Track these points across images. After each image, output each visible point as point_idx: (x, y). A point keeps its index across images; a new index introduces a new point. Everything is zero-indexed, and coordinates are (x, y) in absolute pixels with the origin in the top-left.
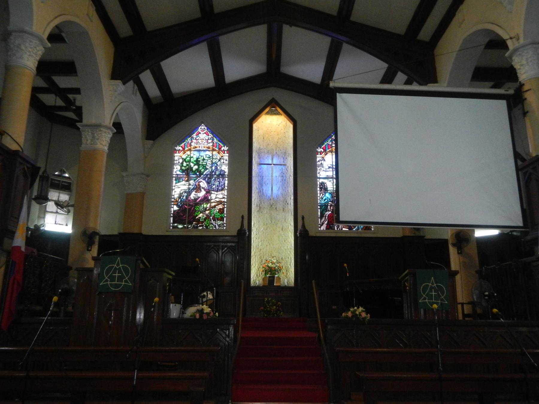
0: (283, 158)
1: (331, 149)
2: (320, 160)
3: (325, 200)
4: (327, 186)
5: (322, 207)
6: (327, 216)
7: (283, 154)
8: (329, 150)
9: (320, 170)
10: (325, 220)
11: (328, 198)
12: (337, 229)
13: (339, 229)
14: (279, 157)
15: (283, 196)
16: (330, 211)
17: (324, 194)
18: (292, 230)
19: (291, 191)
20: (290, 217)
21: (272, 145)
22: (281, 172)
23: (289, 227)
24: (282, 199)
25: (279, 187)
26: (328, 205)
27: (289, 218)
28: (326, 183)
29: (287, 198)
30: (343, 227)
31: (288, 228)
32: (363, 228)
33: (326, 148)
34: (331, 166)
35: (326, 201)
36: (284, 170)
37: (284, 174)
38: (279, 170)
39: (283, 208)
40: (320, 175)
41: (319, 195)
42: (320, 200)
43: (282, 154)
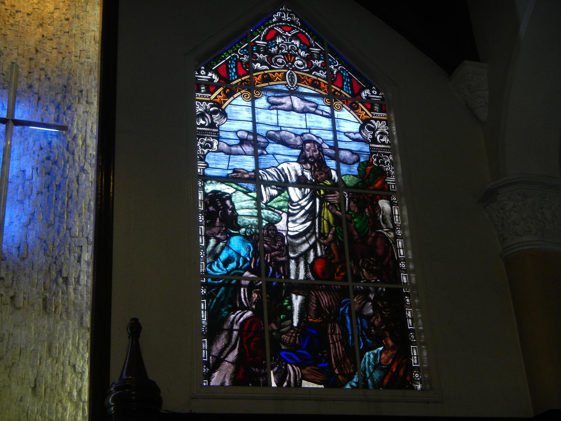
0: (58, 107)
1: (248, 77)
2: (207, 111)
3: (226, 263)
4: (234, 209)
5: (217, 292)
6: (236, 327)
7: (57, 94)
8: (240, 80)
9: (206, 147)
10: (226, 346)
11: (239, 254)
12: (280, 383)
13: (285, 384)
14: (41, 102)
15: (45, 250)
16: (248, 309)
17: (222, 241)
18: (80, 392)
19: (82, 230)
20: (71, 334)
21: (15, 55)
22: (45, 156)
23: (68, 380)
24: (40, 259)
25: (33, 214)
26: (239, 282)
27: (66, 341)
28: (230, 198)
29: (63, 258)
30: (304, 378)
31: (63, 382)
32: (382, 378)
33: (229, 73)
34: (251, 137)
35: (232, 265)
36: (56, 151)
37: (55, 163)
38: (37, 148)
39: (45, 300)
40: (207, 167)
41: (202, 240)
42: (205, 261)
43: (54, 94)
